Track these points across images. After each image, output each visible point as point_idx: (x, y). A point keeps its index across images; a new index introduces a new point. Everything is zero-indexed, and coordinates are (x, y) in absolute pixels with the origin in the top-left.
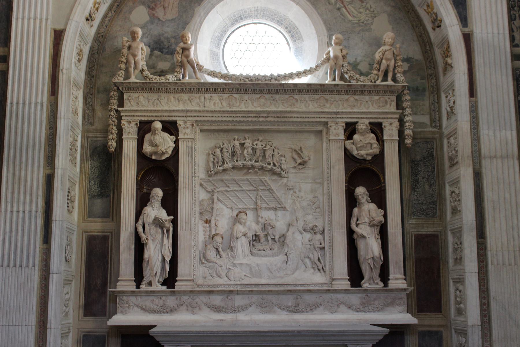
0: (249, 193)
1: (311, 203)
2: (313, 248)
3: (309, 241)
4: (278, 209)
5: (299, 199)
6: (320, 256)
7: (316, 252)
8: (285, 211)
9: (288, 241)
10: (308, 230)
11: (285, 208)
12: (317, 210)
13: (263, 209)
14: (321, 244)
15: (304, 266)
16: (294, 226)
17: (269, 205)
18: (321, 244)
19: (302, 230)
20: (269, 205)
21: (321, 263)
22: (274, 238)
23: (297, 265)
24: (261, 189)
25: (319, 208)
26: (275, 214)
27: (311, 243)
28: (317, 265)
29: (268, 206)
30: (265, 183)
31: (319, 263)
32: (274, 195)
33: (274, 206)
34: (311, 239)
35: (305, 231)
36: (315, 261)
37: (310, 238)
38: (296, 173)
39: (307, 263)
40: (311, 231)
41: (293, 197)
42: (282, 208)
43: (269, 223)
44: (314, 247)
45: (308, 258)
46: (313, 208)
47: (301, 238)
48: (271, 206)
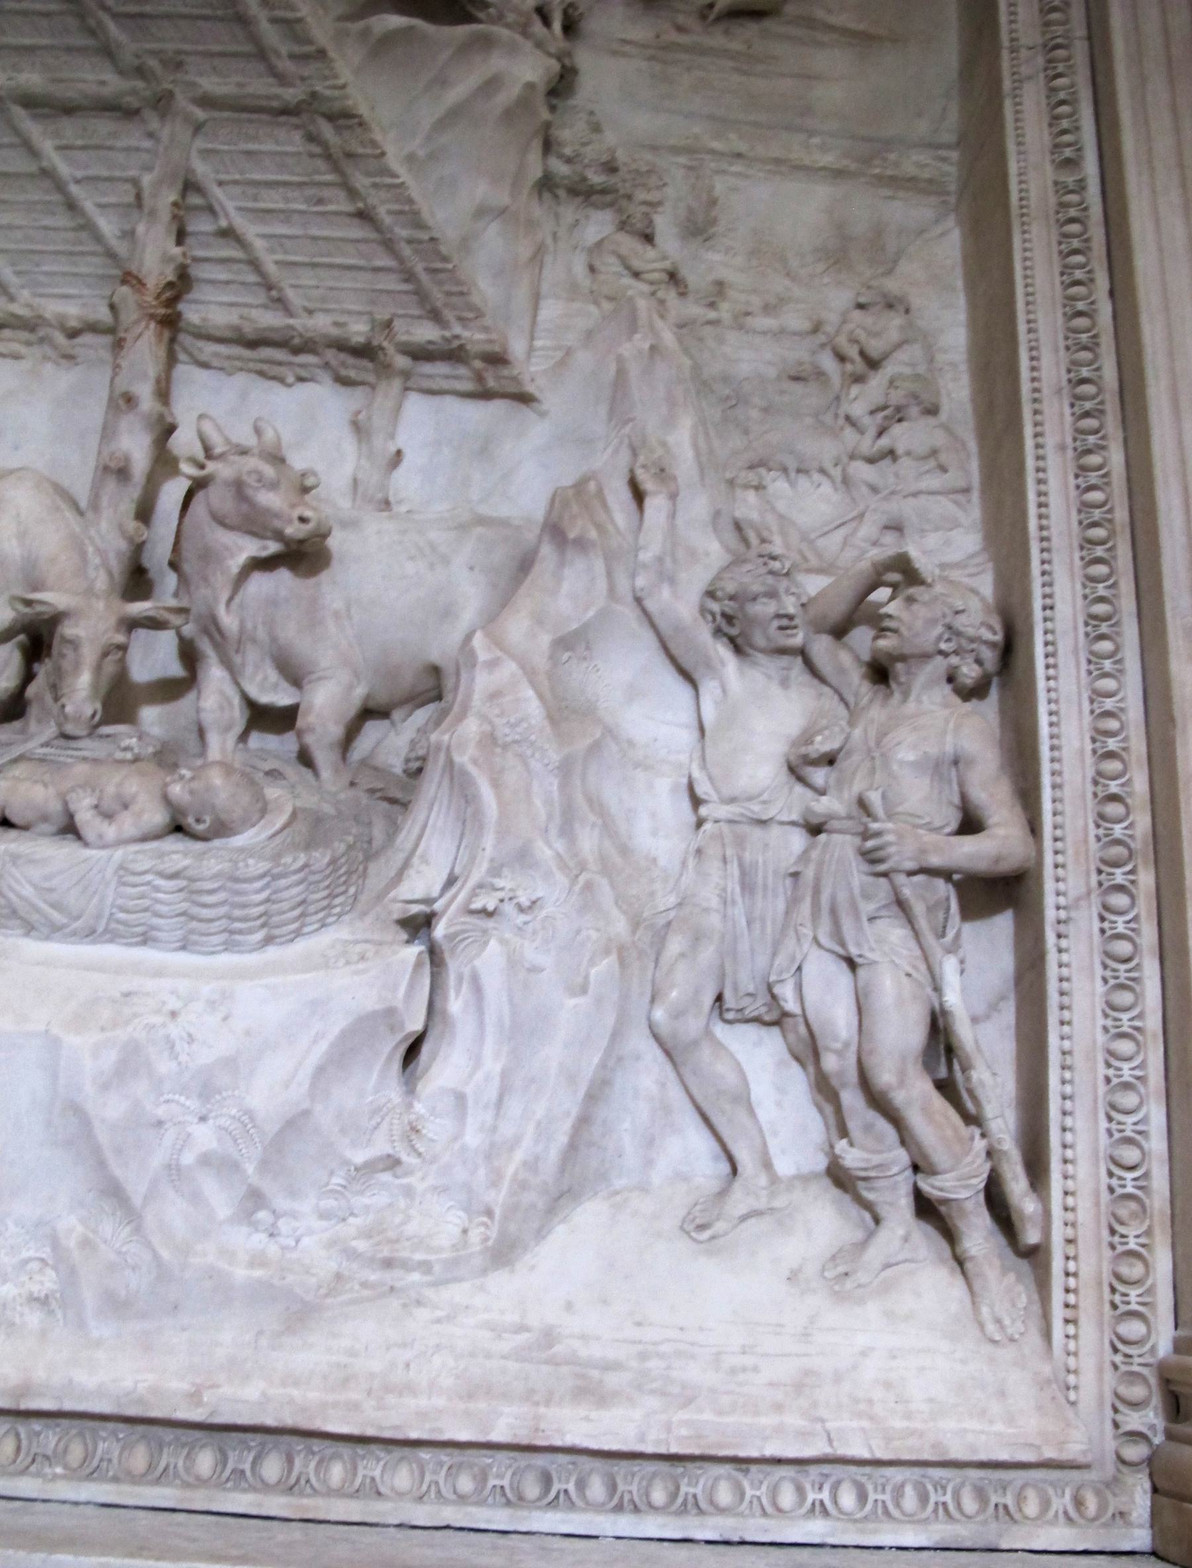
0: (47, 146)
1: (828, 363)
2: (858, 874)
3: (796, 771)
4: (402, 362)
5: (680, 308)
6: (953, 998)
7: (895, 933)
8: (498, 407)
9: (471, 727)
10: (787, 622)
11: (497, 359)
12: (901, 436)
13: (209, 349)
14: (970, 824)
15: (699, 1142)
16: (581, 544)
17: (280, 303)
18: (970, 824)
19: (704, 633)
20: (280, 303)
21: (972, 1119)
22: (282, 698)
23: (584, 1121)
24: (207, 101)
25: (932, 411)
26: (359, 429)
27: (825, 805)
28: (905, 1136)
29: (270, 319)
30: (271, 35)
31: (938, 1102)
32: (361, 181)
33: (358, 330)
34: (822, 745)
35: (738, 648)
36: (885, 1077)
37: (807, 737)
38: (659, 52)
39: (743, 1099)
40: (821, 647)
41: (610, 265)
42: (454, 354)
43: (238, 487)
44: (871, 857)
45: (779, 1020)
46: (858, 409)
47: (686, 737)
48: (321, 324)
